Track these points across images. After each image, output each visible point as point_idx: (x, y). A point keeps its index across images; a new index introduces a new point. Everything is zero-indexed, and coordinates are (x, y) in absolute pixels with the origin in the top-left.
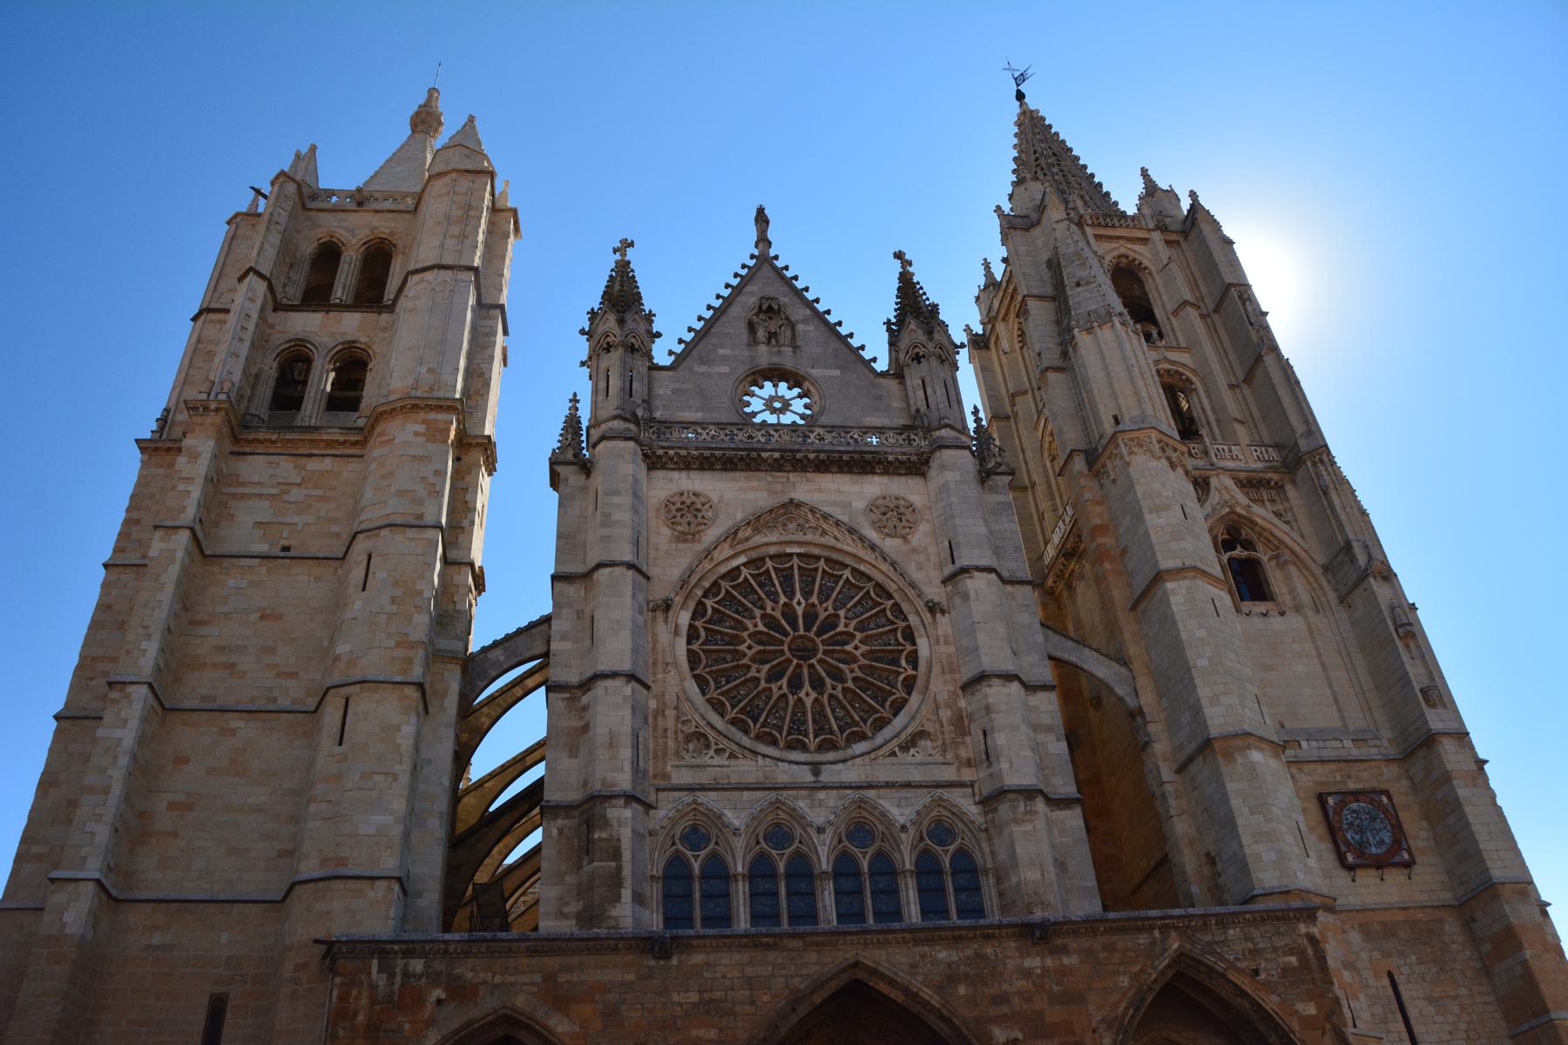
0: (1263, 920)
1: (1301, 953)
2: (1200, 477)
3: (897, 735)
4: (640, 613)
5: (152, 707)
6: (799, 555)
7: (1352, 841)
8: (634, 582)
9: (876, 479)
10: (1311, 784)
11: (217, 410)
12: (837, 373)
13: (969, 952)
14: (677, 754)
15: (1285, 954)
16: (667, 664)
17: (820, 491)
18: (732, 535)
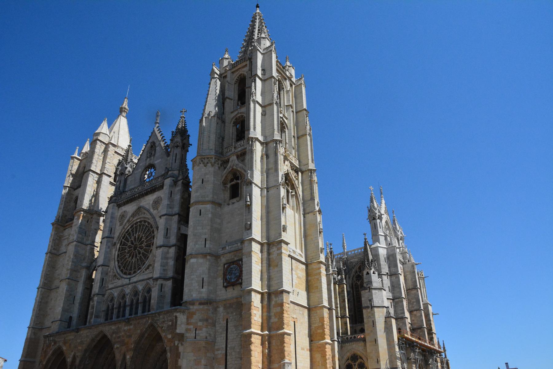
0: (167, 313)
1: (172, 321)
2: (227, 159)
3: (144, 267)
4: (108, 248)
5: (45, 291)
6: (140, 221)
7: (228, 279)
8: (107, 241)
9: (157, 193)
10: (225, 261)
11: (55, 224)
12: (160, 160)
13: (117, 326)
14: (111, 280)
15: (169, 322)
16: (113, 259)
17: (145, 201)
18: (128, 221)
